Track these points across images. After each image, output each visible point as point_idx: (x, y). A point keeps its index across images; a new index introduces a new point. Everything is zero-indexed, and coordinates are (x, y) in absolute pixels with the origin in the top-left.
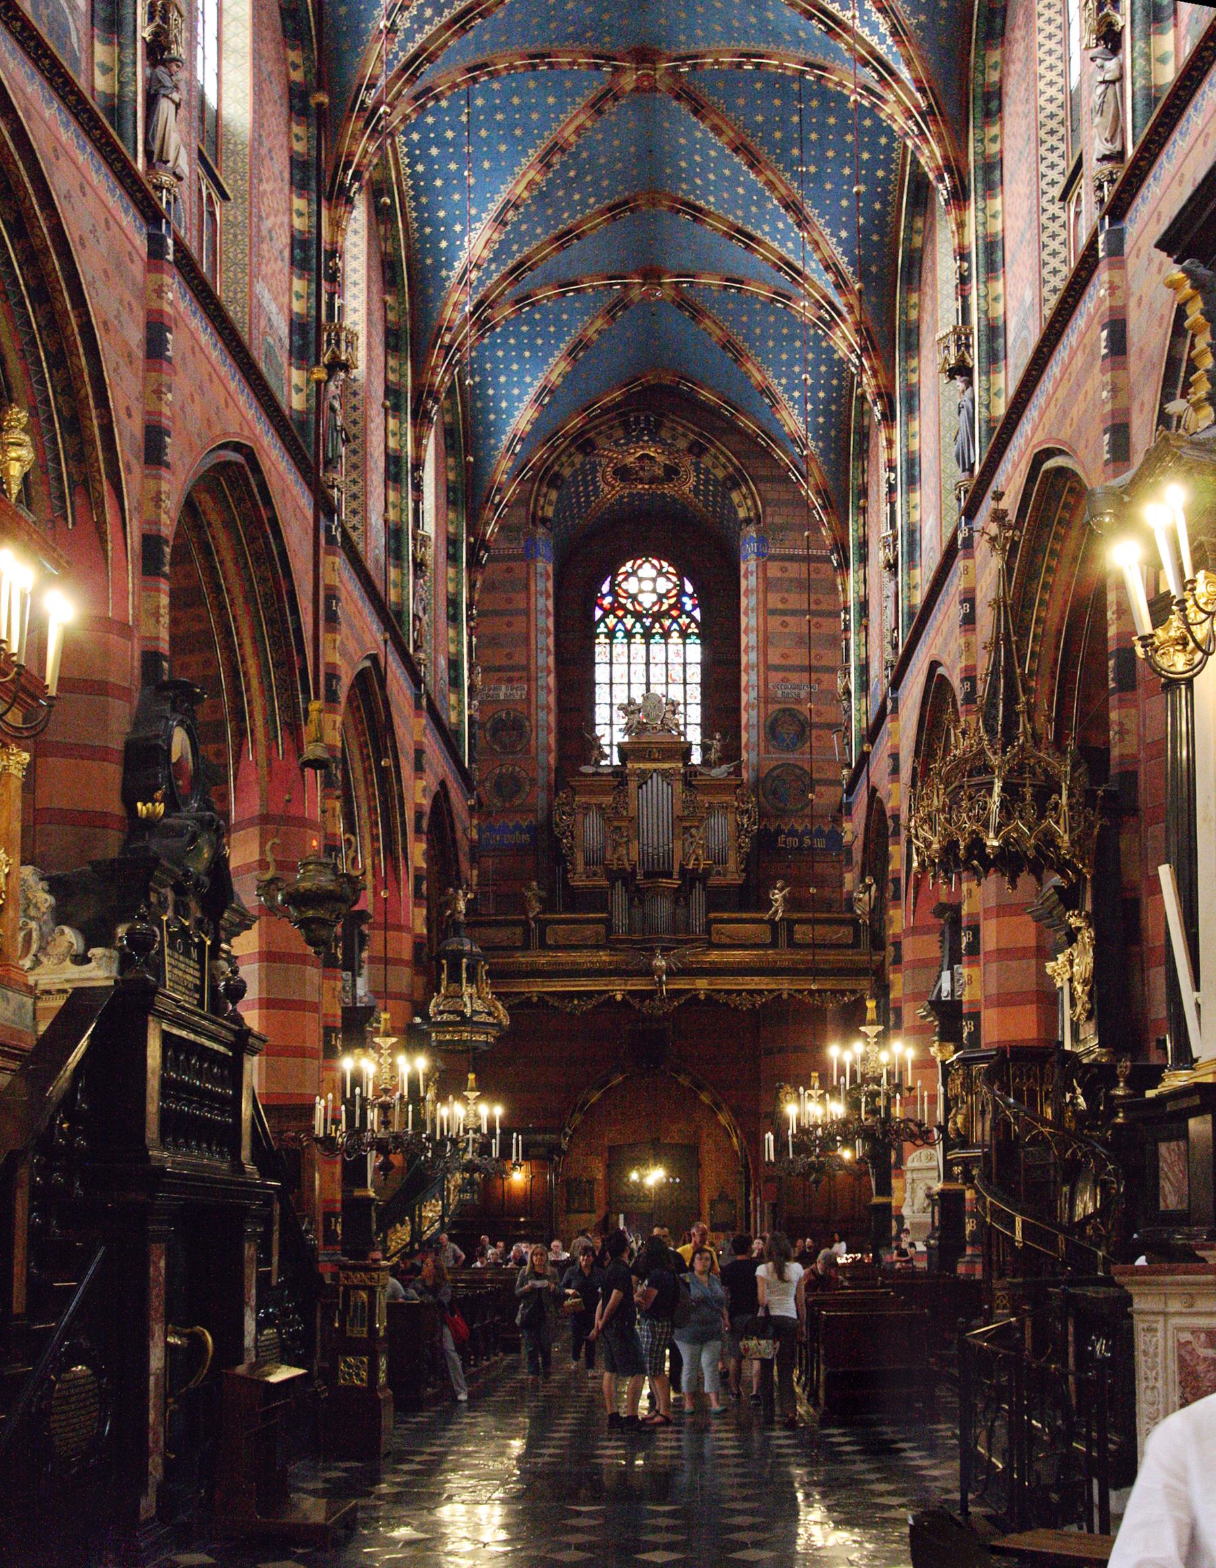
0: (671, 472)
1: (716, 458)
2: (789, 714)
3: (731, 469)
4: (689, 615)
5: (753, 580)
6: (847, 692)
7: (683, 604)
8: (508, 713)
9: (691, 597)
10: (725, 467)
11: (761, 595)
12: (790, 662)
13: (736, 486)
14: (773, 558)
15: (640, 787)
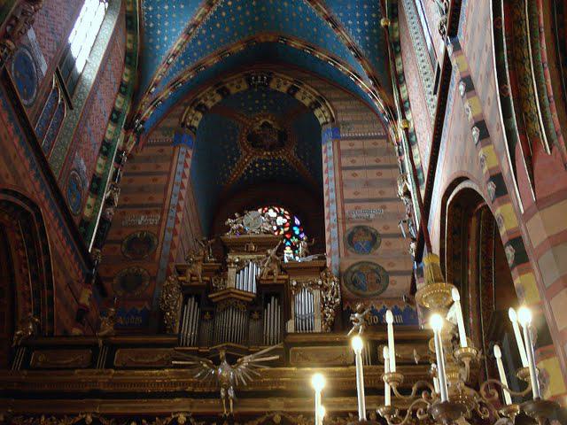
0: (283, 137)
1: (304, 93)
2: (365, 229)
3: (314, 98)
4: (297, 237)
5: (330, 152)
6: (407, 193)
7: (294, 231)
8: (142, 233)
9: (298, 227)
10: (310, 98)
11: (337, 159)
12: (360, 197)
13: (317, 105)
14: (345, 139)
15: (238, 272)
